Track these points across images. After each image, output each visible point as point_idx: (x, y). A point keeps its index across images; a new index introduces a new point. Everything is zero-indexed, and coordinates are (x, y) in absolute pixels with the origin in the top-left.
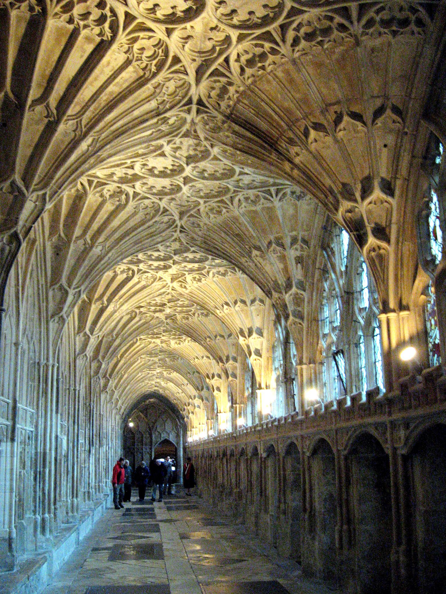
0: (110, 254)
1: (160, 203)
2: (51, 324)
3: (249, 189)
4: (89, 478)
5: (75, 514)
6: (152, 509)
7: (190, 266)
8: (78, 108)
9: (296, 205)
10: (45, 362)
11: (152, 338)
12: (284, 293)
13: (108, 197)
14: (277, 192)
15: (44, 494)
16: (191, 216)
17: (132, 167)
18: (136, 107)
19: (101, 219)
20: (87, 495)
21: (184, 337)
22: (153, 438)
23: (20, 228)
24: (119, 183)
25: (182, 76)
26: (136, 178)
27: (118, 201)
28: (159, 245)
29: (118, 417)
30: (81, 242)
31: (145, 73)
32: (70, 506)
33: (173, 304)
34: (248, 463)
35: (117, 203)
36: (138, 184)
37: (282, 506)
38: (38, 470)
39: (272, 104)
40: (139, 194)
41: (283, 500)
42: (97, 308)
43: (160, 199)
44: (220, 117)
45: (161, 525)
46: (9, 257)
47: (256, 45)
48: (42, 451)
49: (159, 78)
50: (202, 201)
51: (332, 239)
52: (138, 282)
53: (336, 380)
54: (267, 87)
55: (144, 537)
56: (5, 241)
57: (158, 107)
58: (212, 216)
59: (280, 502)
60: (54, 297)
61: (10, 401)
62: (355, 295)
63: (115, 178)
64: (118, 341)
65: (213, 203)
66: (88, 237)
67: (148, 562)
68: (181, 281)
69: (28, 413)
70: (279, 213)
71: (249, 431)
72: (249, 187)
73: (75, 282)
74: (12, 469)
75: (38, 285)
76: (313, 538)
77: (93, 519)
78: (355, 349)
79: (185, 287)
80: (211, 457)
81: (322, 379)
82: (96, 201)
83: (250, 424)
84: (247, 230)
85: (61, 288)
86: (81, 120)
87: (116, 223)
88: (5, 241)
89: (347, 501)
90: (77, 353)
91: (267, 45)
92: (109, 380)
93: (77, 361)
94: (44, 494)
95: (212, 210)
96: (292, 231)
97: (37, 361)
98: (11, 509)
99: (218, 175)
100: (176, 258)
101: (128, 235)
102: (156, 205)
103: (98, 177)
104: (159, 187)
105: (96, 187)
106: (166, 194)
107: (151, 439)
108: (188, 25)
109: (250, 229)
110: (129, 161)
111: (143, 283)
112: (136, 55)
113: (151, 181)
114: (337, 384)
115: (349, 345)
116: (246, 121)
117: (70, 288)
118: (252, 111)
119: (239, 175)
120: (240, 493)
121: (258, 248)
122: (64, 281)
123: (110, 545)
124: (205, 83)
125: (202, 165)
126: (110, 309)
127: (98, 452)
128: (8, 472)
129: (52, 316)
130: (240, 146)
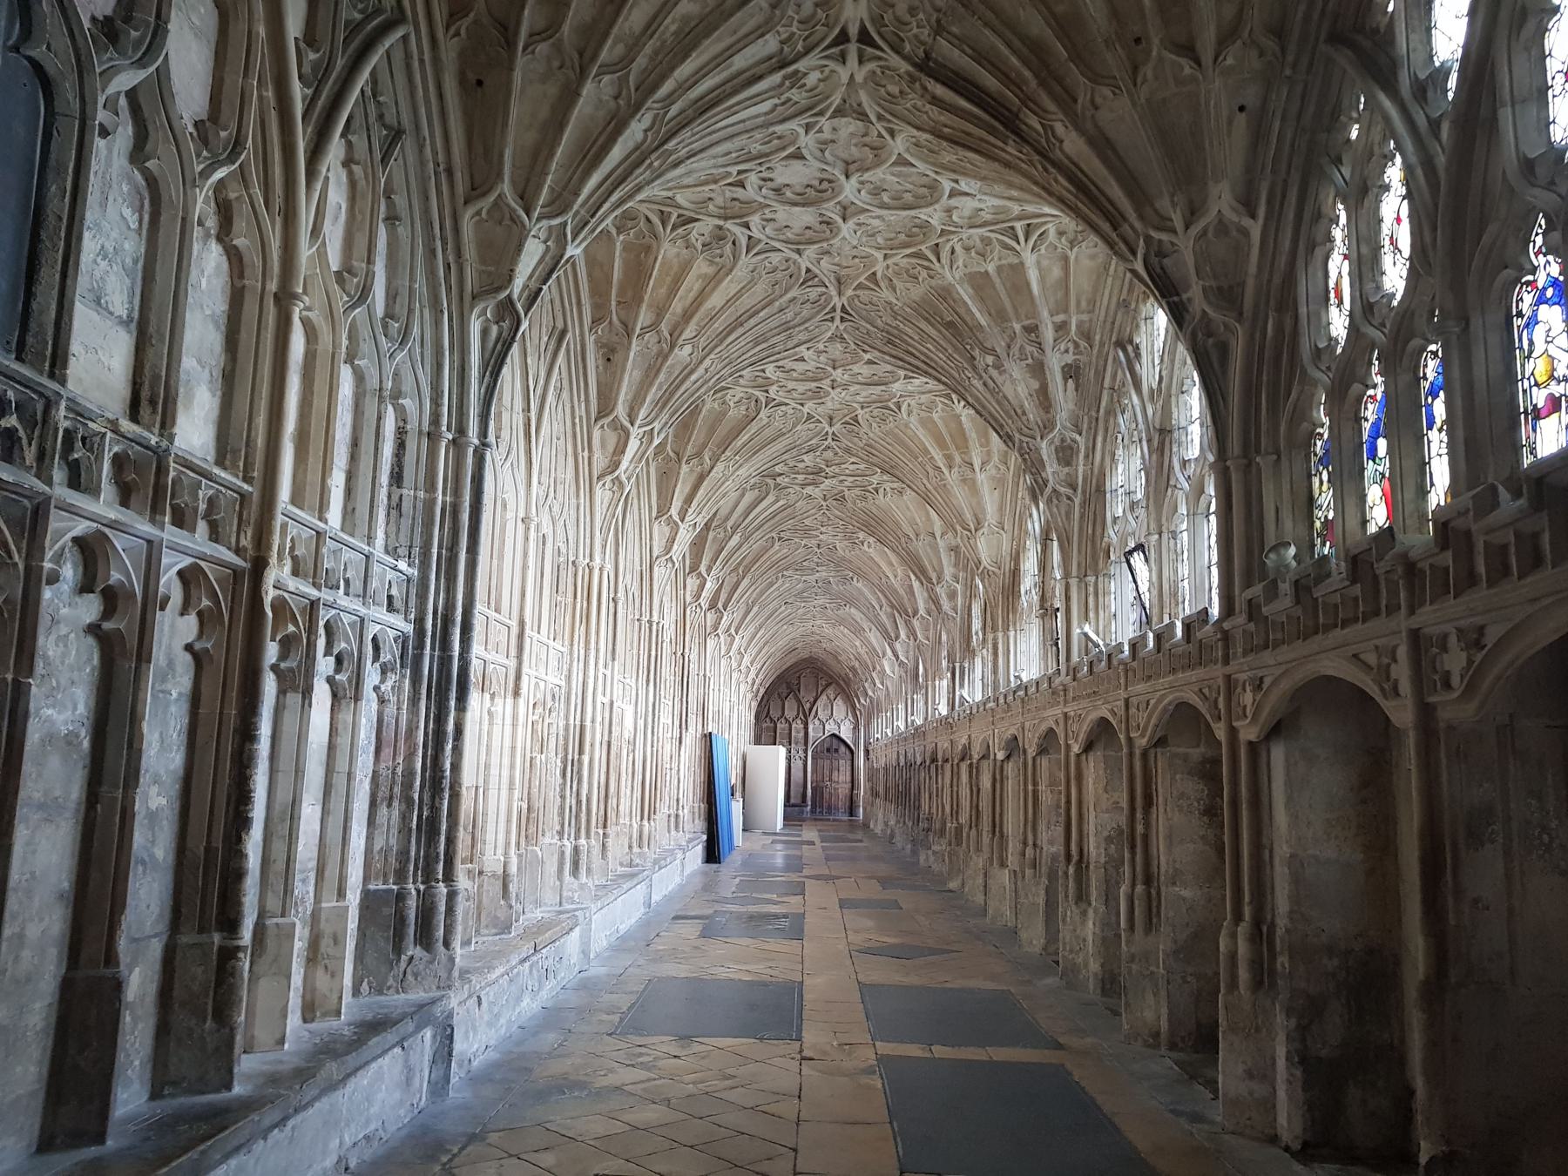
0: (707, 362)
2: (598, 492)
3: (971, 227)
8: (620, 49)
9: (1066, 259)
10: (587, 560)
13: (700, 247)
15: (579, 802)
16: (860, 286)
18: (738, 46)
20: (673, 819)
21: (861, 535)
22: (810, 730)
24: (719, 217)
26: (749, 207)
28: (803, 348)
34: (974, 771)
36: (755, 220)
37: (1029, 851)
38: (570, 757)
40: (760, 241)
41: (1030, 842)
42: (692, 471)
44: (904, 67)
46: (499, 347)
48: (578, 723)
50: (879, 255)
51: (1138, 326)
52: (768, 425)
59: (1025, 843)
61: (514, 624)
62: (1176, 435)
64: (736, 539)
65: (900, 259)
66: (664, 328)
69: (551, 650)
70: (1033, 276)
71: (974, 711)
73: (642, 413)
74: (513, 748)
75: (573, 418)
76: (1084, 913)
78: (1172, 541)
80: (910, 765)
82: (678, 255)
83: (978, 697)
85: (616, 426)
87: (716, 300)
89: (1146, 837)
90: (655, 555)
93: (656, 569)
94: (579, 802)
97: (571, 559)
98: (509, 821)
99: (908, 197)
103: (680, 207)
107: (806, 734)
109: (974, 310)
110: (734, 170)
113: (782, 213)
114: (1134, 615)
119: (950, 196)
120: (959, 830)
122: (621, 410)
125: (878, 175)
128: (507, 751)
130: (946, 130)
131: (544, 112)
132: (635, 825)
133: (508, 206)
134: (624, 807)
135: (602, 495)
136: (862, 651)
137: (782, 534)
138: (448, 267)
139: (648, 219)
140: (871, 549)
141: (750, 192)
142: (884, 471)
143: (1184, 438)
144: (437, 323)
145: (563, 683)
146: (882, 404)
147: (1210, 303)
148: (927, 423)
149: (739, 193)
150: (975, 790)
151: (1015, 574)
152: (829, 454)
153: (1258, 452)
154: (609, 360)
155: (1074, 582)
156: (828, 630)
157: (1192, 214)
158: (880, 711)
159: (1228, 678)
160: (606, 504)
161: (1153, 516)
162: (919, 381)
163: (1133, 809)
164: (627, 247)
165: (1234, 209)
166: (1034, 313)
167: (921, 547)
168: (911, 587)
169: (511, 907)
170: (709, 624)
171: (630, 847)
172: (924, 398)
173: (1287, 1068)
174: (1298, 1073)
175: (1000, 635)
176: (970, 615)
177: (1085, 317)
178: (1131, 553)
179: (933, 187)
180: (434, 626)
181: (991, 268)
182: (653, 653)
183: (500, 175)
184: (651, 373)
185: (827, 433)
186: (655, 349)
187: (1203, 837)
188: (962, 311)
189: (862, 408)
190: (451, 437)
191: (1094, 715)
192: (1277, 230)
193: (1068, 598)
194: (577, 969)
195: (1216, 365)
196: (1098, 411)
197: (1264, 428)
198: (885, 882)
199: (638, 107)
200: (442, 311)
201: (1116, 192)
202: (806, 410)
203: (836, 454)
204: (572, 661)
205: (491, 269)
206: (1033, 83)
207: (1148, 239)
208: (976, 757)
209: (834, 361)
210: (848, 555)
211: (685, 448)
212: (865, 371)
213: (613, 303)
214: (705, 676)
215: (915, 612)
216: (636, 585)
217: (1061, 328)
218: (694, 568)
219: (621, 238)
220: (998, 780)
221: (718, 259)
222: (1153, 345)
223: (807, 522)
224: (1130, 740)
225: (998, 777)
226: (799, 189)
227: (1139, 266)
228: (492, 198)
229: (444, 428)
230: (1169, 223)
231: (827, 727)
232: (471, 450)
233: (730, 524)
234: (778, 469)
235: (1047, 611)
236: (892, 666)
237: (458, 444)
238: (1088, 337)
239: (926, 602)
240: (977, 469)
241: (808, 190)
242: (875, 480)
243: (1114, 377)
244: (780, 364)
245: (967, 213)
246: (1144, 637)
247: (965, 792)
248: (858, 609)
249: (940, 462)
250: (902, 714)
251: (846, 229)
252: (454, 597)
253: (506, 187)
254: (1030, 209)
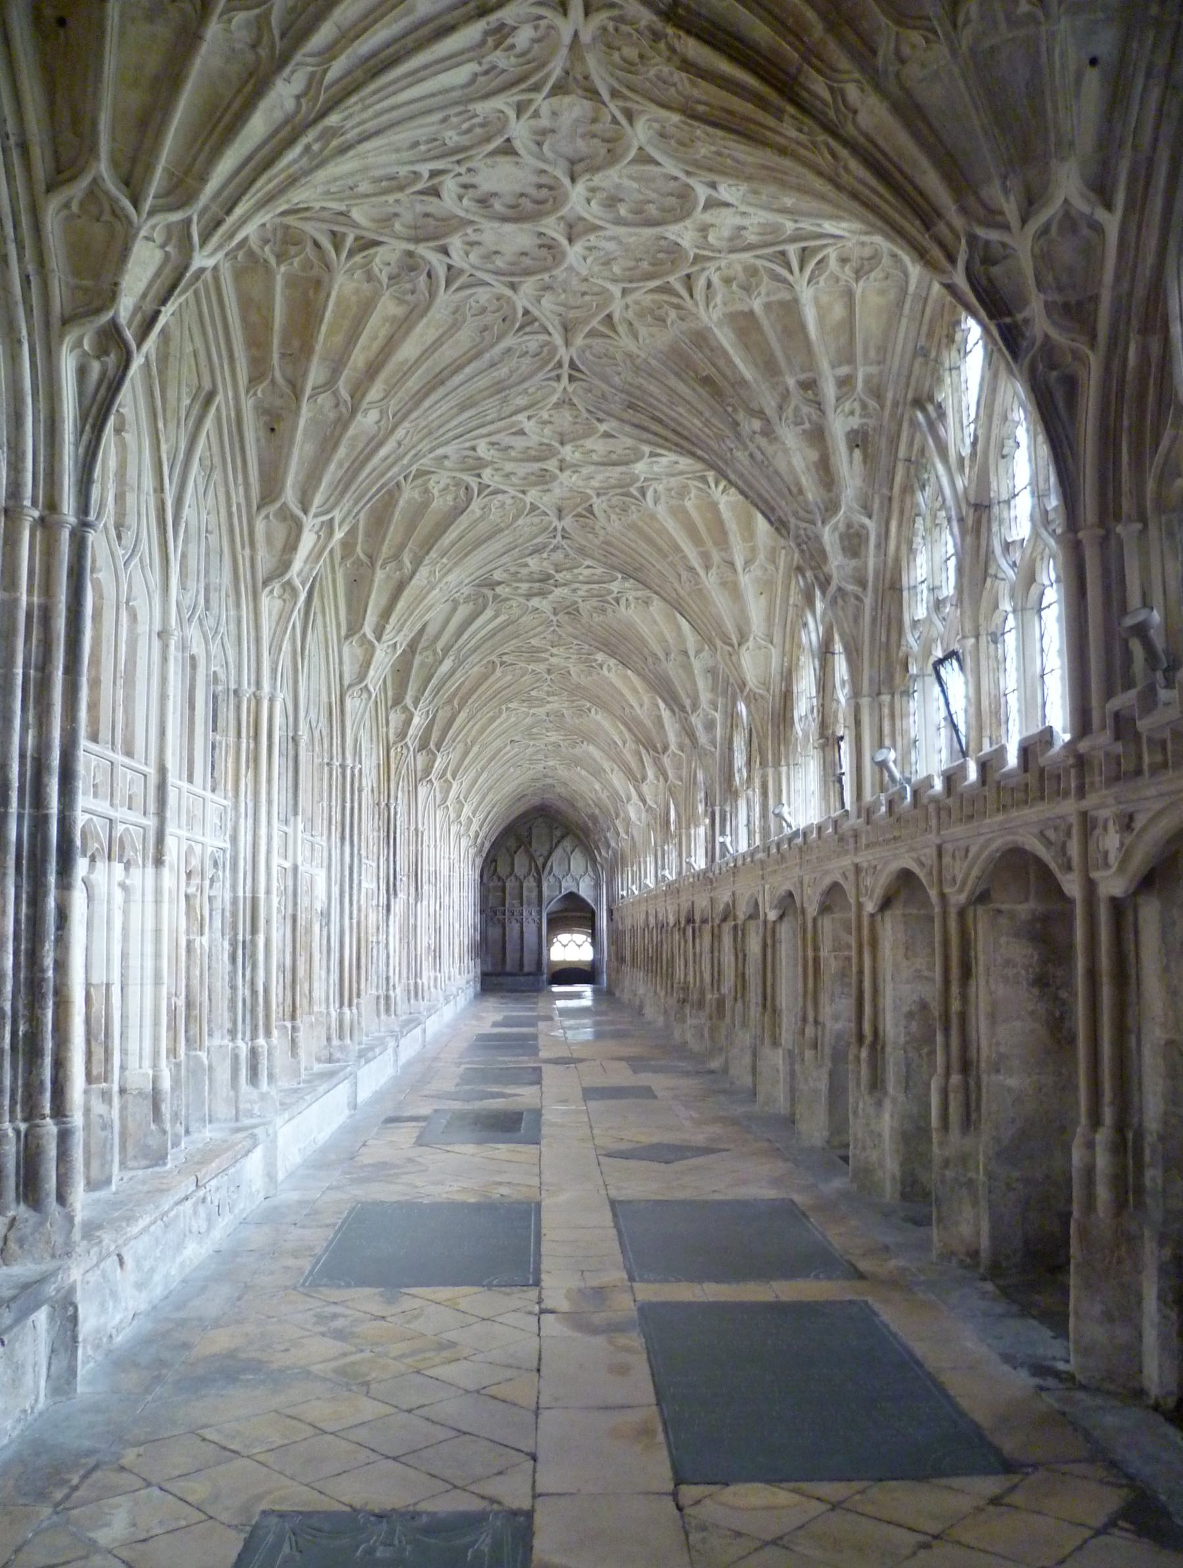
0: (400, 433)
1: (515, 297)
2: (265, 600)
3: (732, 251)
4: (388, 965)
5: (348, 1041)
6: (535, 1037)
10: (253, 689)
11: (529, 662)
12: (819, 523)
13: (385, 280)
14: (804, 256)
15: (254, 993)
16: (592, 334)
17: (435, 192)
19: (376, 338)
20: (382, 1001)
21: (600, 657)
22: (545, 888)
23: (125, 307)
24: (409, 240)
28: (521, 417)
29: (464, 842)
32: (334, 1025)
34: (739, 933)
36: (455, 243)
37: (810, 1030)
38: (240, 938)
41: (811, 1018)
42: (389, 577)
45: (545, 1067)
46: (103, 391)
48: (248, 895)
50: (616, 290)
52: (482, 518)
53: (943, 731)
55: (502, 1095)
56: (86, 347)
58: (643, 331)
59: (804, 1020)
61: (152, 771)
64: (447, 665)
65: (643, 295)
67: (503, 1150)
68: (579, 515)
69: (209, 805)
71: (740, 862)
73: (318, 500)
74: (157, 931)
75: (229, 506)
77: (396, 1053)
78: (992, 646)
80: (662, 926)
81: (908, 732)
82: (357, 292)
83: (743, 847)
84: (730, 362)
85: (285, 514)
87: (408, 350)
88: (86, 347)
90: (346, 683)
92: (435, 755)
93: (348, 701)
94: (254, 993)
95: (641, 315)
96: (840, 365)
97: (233, 686)
98: (156, 1023)
99: (652, 210)
100: (568, 452)
101: (442, 383)
103: (355, 225)
105: (351, 253)
106: (528, 273)
109: (737, 361)
110: (424, 169)
113: (491, 233)
115: (977, 637)
116: (713, 23)
117: (305, 512)
119: (707, 207)
120: (721, 1003)
123: (425, 1110)
125: (612, 177)
127: (410, 913)
129: (265, 583)
130: (701, 108)
131: (153, 63)
132: (334, 1014)
133: (107, 193)
134: (319, 992)
135: (269, 604)
136: (604, 796)
137: (505, 658)
138: (26, 280)
139: (317, 245)
140: (612, 672)
141: (450, 201)
142: (627, 576)
143: (1005, 514)
145: (228, 845)
146: (623, 487)
147: (1055, 324)
148: (680, 513)
149: (432, 205)
150: (741, 954)
151: (787, 698)
152: (558, 556)
153: (1118, 518)
154: (273, 430)
155: (865, 702)
156: (562, 772)
157: (1031, 202)
158: (624, 864)
159: (1084, 815)
160: (275, 617)
161: (968, 613)
162: (668, 458)
163: (947, 982)
164: (292, 282)
165: (1083, 196)
166: (810, 363)
167: (671, 668)
168: (659, 718)
169: (164, 1132)
170: (419, 768)
171: (329, 1039)
172: (673, 482)
173: (1159, 1311)
174: (1173, 1315)
175: (770, 771)
176: (731, 749)
177: (873, 369)
178: (941, 662)
179: (685, 195)
180: (22, 774)
181: (757, 305)
182: (348, 805)
183: (93, 149)
184: (327, 445)
185: (555, 529)
186: (332, 415)
187: (1032, 1013)
188: (721, 363)
189: (598, 495)
190: (36, 514)
191: (895, 866)
192: (1140, 227)
193: (858, 723)
194: (262, 1195)
195: (1061, 405)
196: (891, 488)
197: (1125, 488)
198: (636, 1063)
199: (282, 61)
200: (19, 342)
201: (932, 182)
202: (528, 499)
203: (567, 556)
204: (237, 817)
205: (88, 283)
206: (818, 29)
207: (972, 239)
208: (741, 916)
209: (561, 434)
210: (584, 681)
211: (380, 550)
212: (599, 446)
213: (276, 356)
214: (416, 829)
215: (665, 748)
216: (323, 721)
217: (845, 383)
218: (398, 700)
219: (283, 269)
220: (769, 944)
221: (409, 297)
222: (960, 402)
223: (534, 642)
224: (943, 896)
225: (769, 941)
226: (510, 200)
227: (960, 279)
228: (84, 183)
229: (27, 502)
230: (999, 218)
231: (564, 884)
232: (65, 535)
233: (440, 645)
234: (498, 575)
235: (829, 741)
236: (639, 811)
237: (47, 525)
238: (878, 396)
239: (678, 735)
240: (739, 569)
241: (522, 200)
242: (615, 587)
243: (911, 444)
244: (494, 439)
245: (726, 233)
246: (963, 768)
247: (728, 959)
248: (598, 747)
249: (696, 562)
250: (651, 868)
251: (574, 253)
252: (49, 732)
253: (103, 167)
254: (807, 225)
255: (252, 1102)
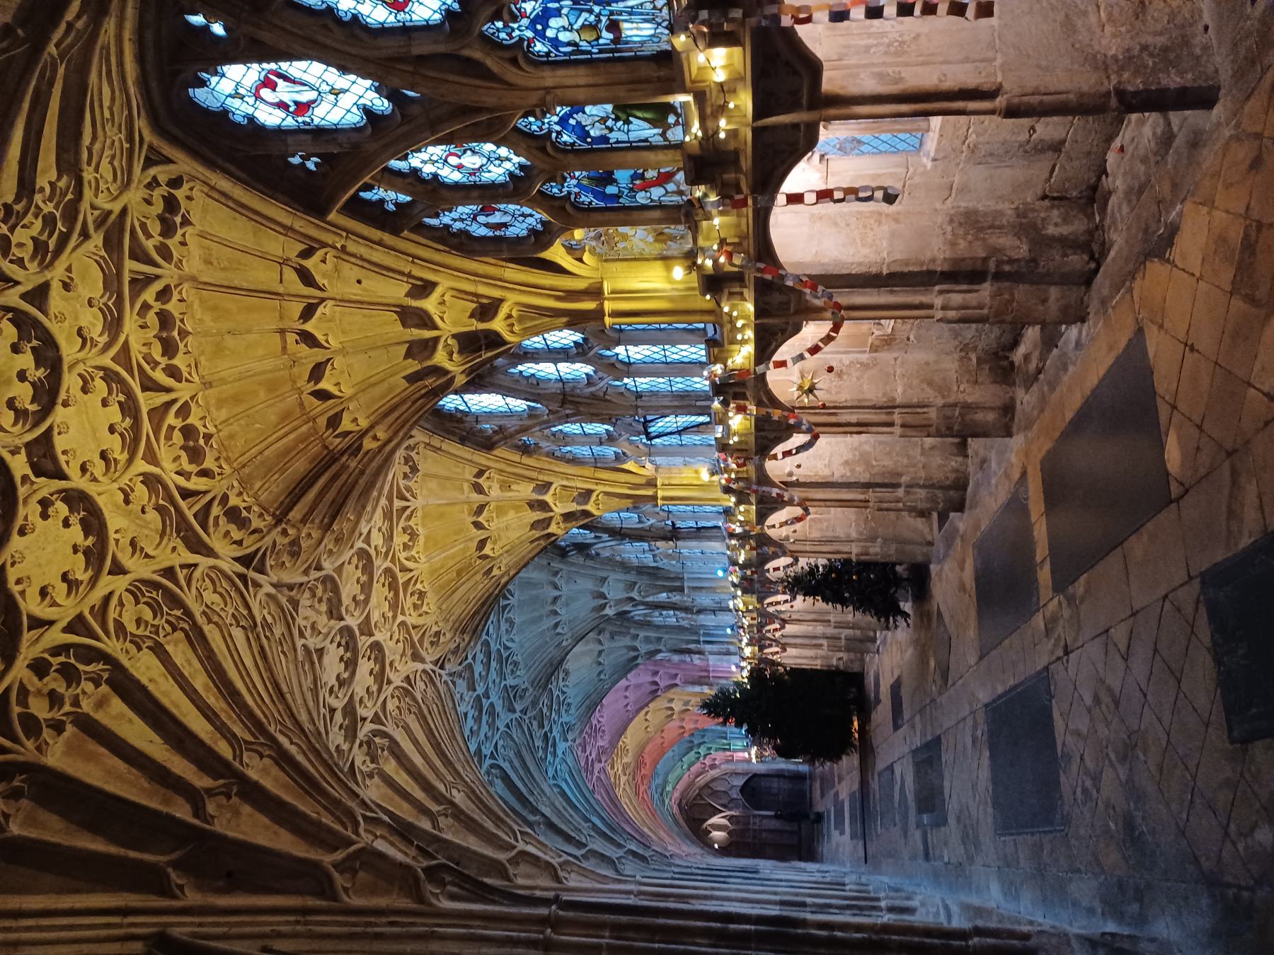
2: (572, 884)
5: (871, 888)
7: (493, 675)
11: (592, 773)
13: (373, 766)
16: (421, 641)
24: (353, 743)
25: (197, 574)
26: (349, 710)
27: (383, 750)
30: (442, 821)
31: (182, 629)
33: (546, 723)
35: (386, 753)
36: (361, 712)
39: (270, 440)
40: (376, 714)
43: (389, 682)
47: (169, 437)
49: (197, 609)
50: (400, 618)
52: (511, 762)
54: (240, 443)
57: (243, 627)
60: (529, 876)
63: (345, 747)
66: (435, 808)
72: (389, 538)
79: (525, 690)
82: (378, 787)
84: (453, 557)
85: (514, 861)
86: (246, 742)
87: (418, 760)
91: (171, 419)
99: (364, 578)
100: (480, 690)
102: (397, 693)
104: (370, 681)
108: (112, 536)
111: (512, 754)
112: (147, 633)
118: (276, 476)
121: (482, 544)
122: (502, 856)
124: (216, 543)
126: (546, 811)
130: (326, 520)
141: (338, 704)
144: (443, 938)
160: (583, 879)
172: (504, 626)
183: (316, 865)
184: (471, 825)
186: (450, 820)
210: (607, 737)
255: (928, 914)
